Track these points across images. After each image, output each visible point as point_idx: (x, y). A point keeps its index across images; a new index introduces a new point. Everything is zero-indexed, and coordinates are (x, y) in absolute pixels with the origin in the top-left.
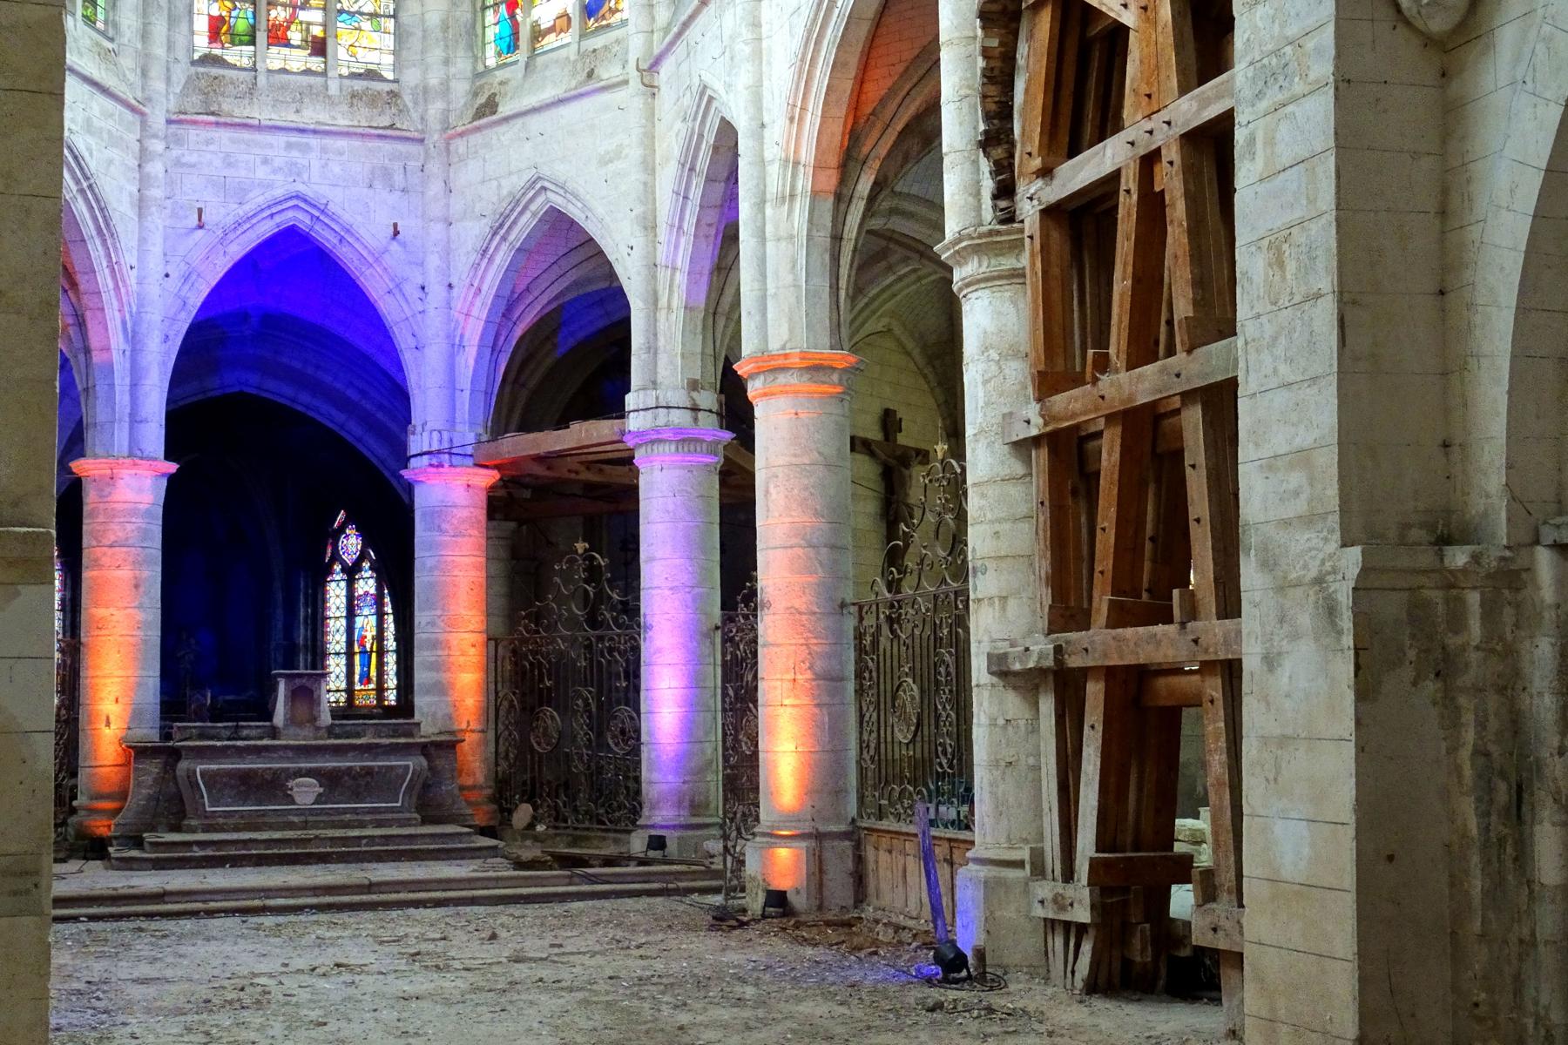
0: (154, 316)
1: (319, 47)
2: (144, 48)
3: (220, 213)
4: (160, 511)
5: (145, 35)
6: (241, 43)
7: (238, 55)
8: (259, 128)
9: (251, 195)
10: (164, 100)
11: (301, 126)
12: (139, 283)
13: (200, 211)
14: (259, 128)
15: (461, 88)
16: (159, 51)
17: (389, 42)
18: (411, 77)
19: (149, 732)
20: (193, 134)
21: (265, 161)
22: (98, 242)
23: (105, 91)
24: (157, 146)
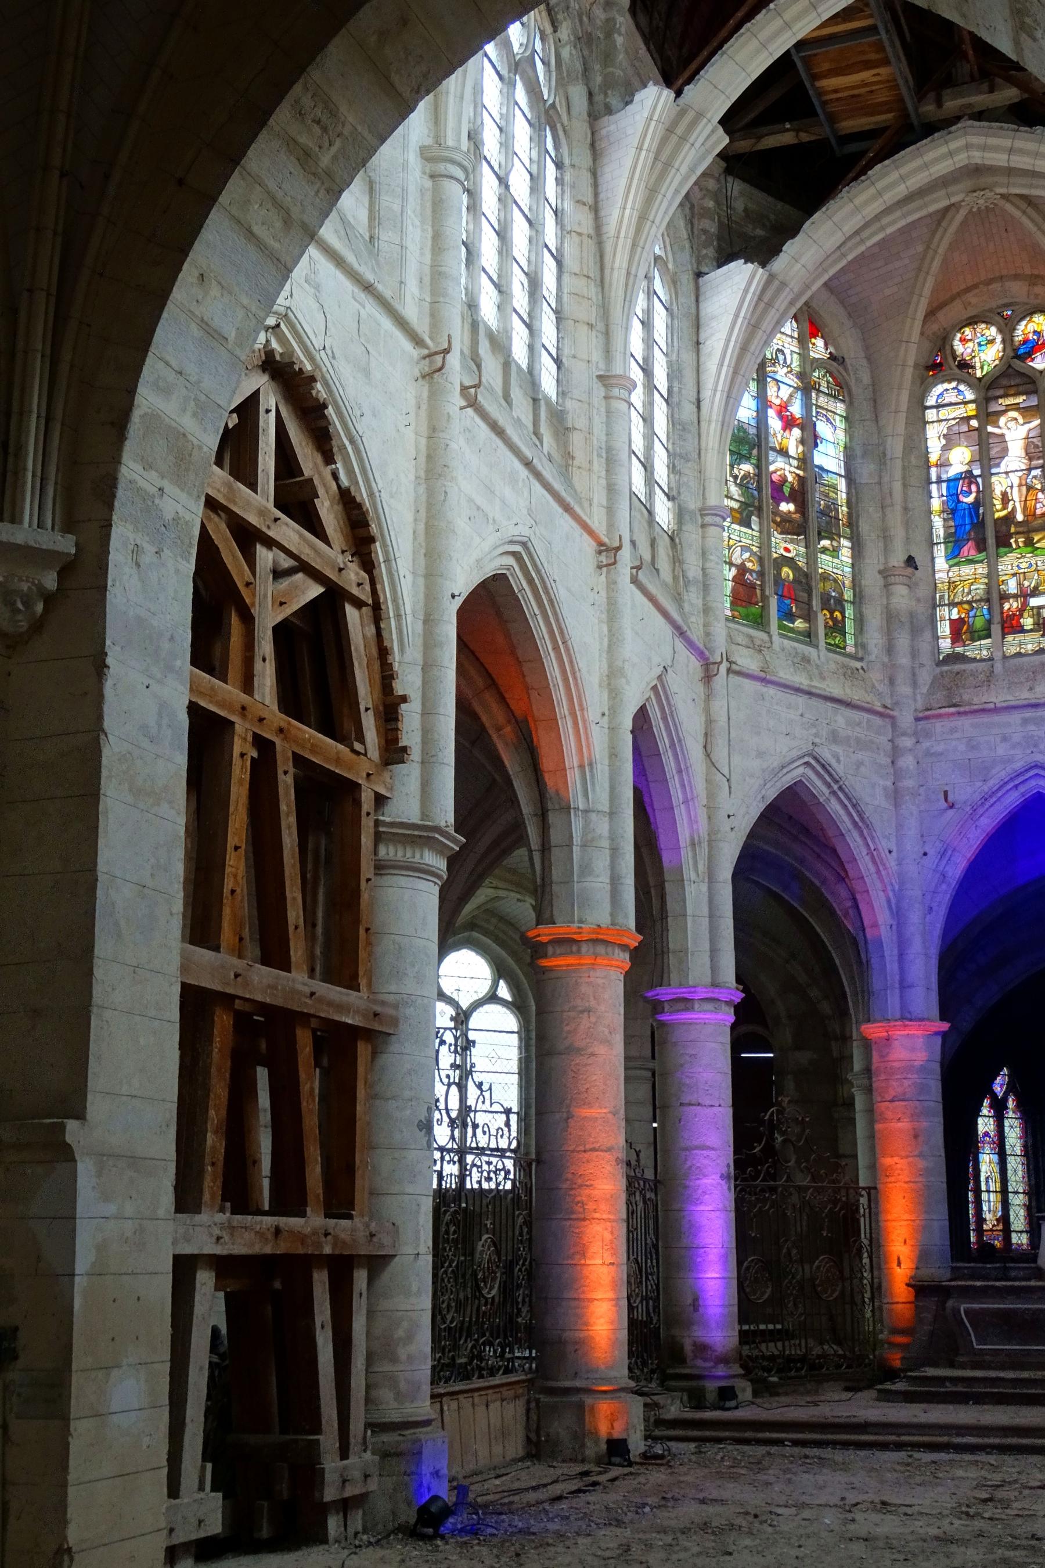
0: (914, 892)
2: (890, 661)
3: (965, 792)
5: (890, 649)
6: (980, 639)
7: (978, 649)
8: (996, 710)
9: (994, 771)
10: (910, 701)
11: (1033, 701)
12: (899, 864)
13: (946, 793)
14: (996, 710)
16: (904, 660)
19: (939, 1272)
20: (939, 726)
21: (1005, 739)
22: (856, 834)
23: (848, 704)
24: (907, 742)
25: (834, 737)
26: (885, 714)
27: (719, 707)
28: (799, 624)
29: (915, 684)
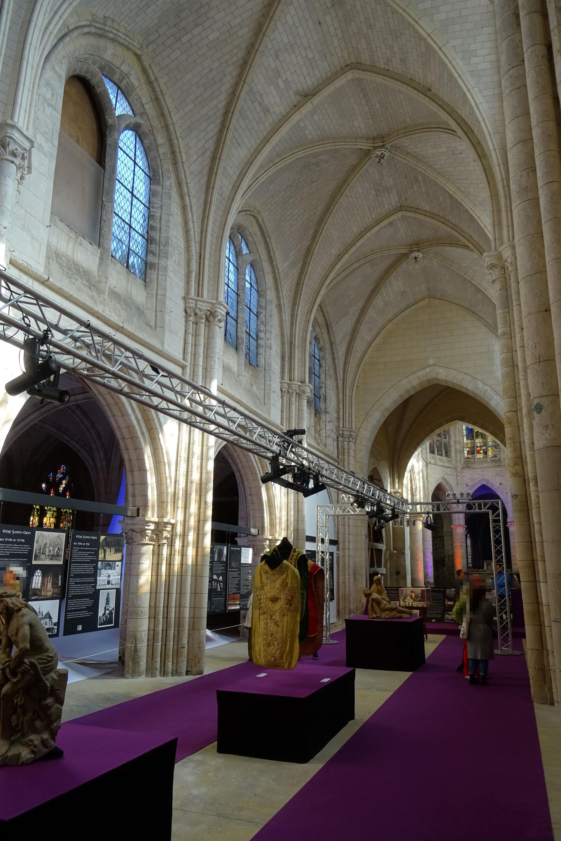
1: (485, 453)
3: (470, 484)
5: (456, 456)
10: (460, 465)
18: (502, 456)
20: (465, 471)
24: (459, 474)
25: (447, 474)
26: (456, 468)
27: (429, 471)
28: (440, 452)
29: (460, 463)
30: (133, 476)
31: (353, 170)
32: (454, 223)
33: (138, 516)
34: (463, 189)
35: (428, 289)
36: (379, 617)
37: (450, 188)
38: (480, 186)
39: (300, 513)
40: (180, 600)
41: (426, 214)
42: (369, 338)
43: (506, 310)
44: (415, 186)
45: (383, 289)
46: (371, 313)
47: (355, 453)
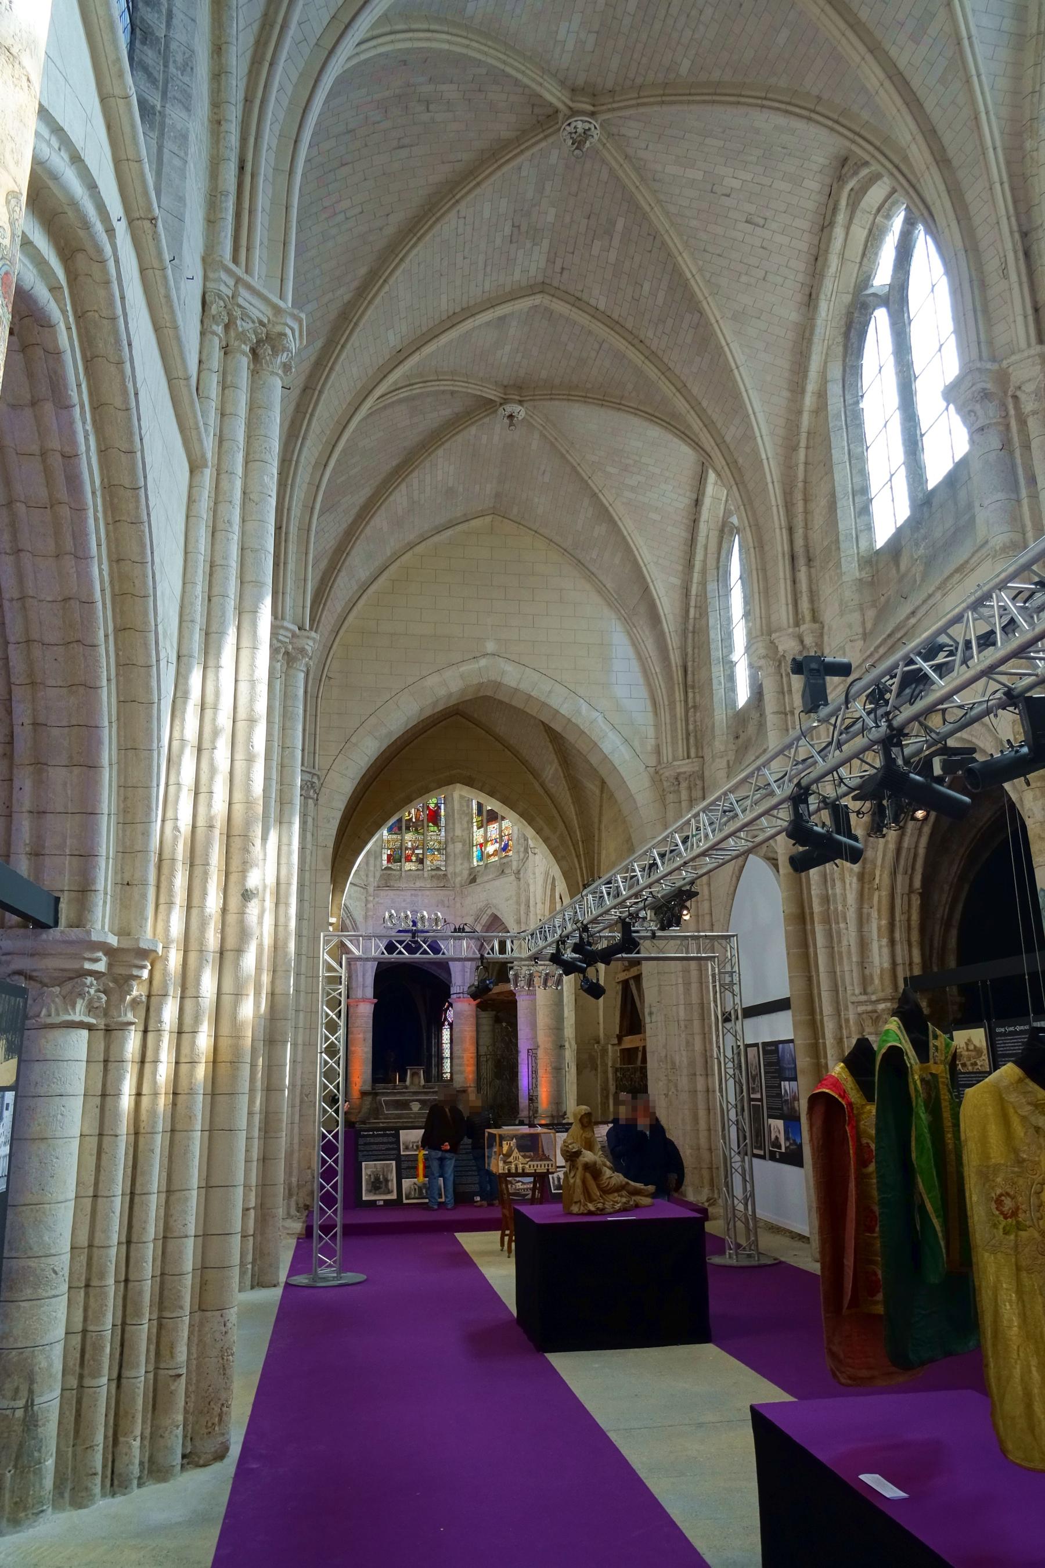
1: (421, 861)
4: (371, 1015)
7: (395, 866)
10: (373, 882)
15: (466, 873)
17: (444, 857)
18: (450, 869)
19: (368, 1087)
20: (382, 893)
24: (371, 898)
26: (365, 887)
30: (40, 782)
31: (495, 155)
32: (654, 348)
33: (56, 924)
34: (708, 275)
35: (498, 495)
36: (601, 1211)
37: (687, 263)
38: (744, 279)
39: (280, 952)
40: (167, 1216)
41: (595, 313)
42: (363, 574)
43: (1013, 496)
44: (597, 244)
45: (415, 474)
46: (380, 521)
47: (316, 826)
